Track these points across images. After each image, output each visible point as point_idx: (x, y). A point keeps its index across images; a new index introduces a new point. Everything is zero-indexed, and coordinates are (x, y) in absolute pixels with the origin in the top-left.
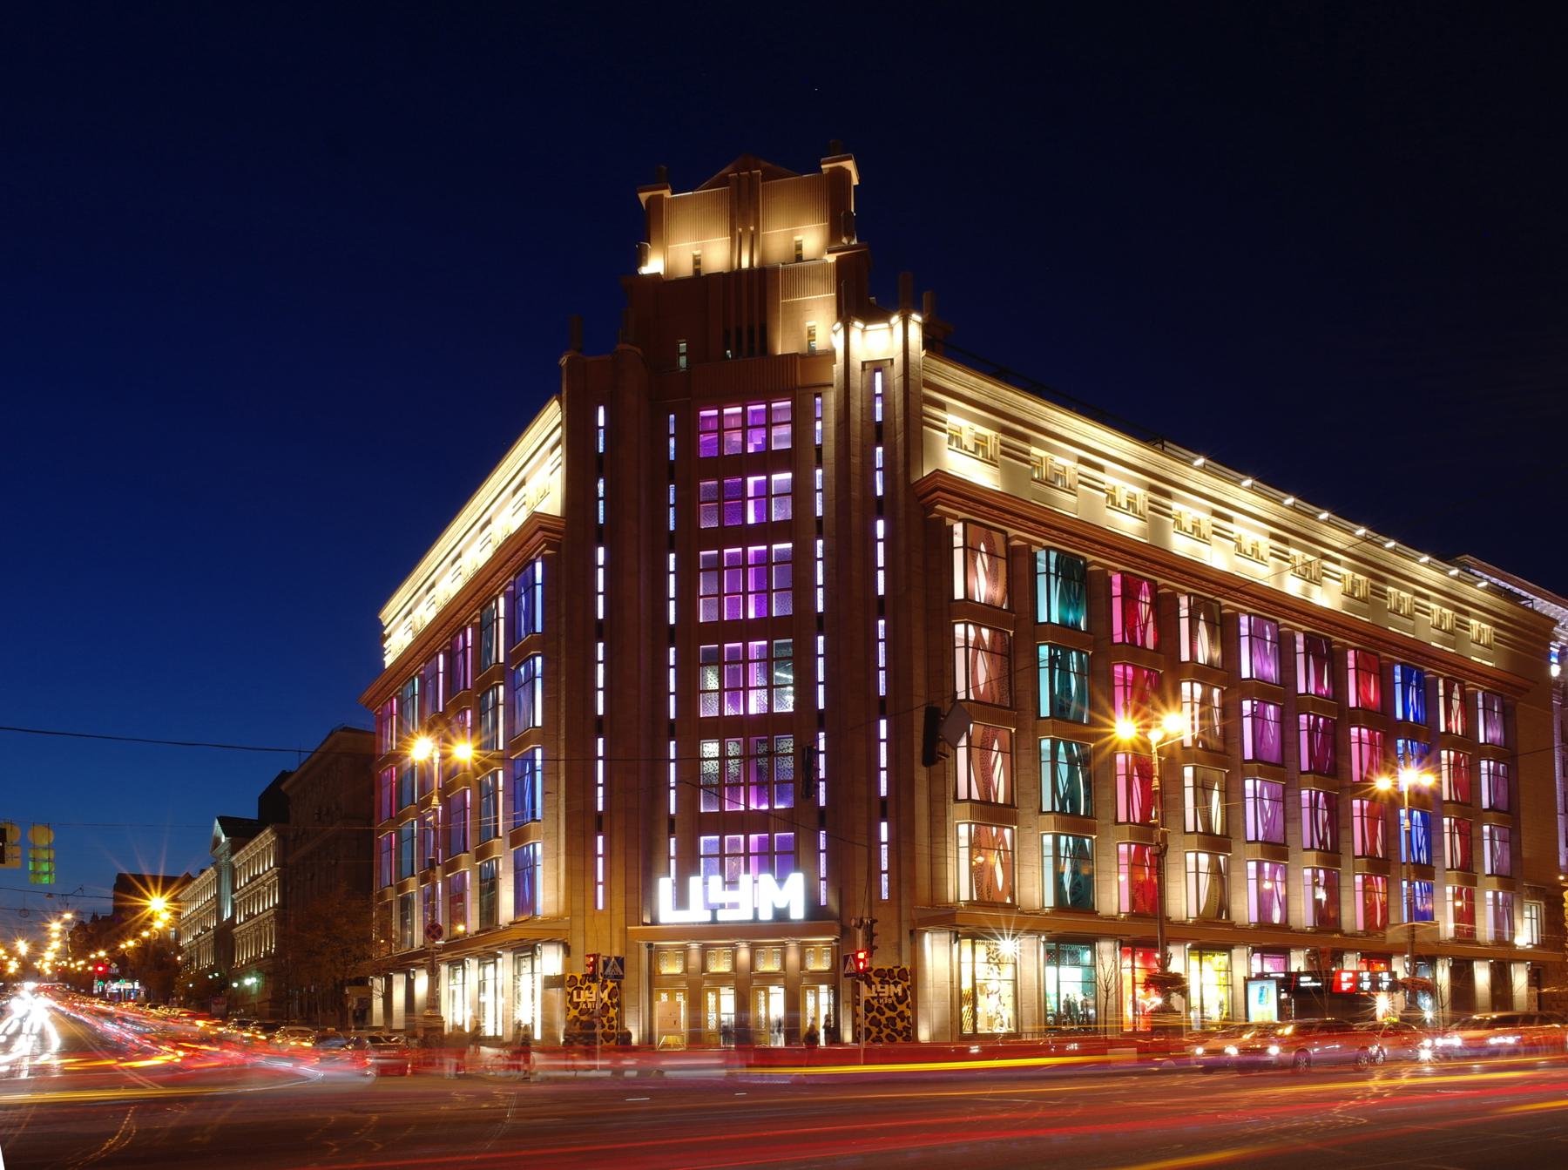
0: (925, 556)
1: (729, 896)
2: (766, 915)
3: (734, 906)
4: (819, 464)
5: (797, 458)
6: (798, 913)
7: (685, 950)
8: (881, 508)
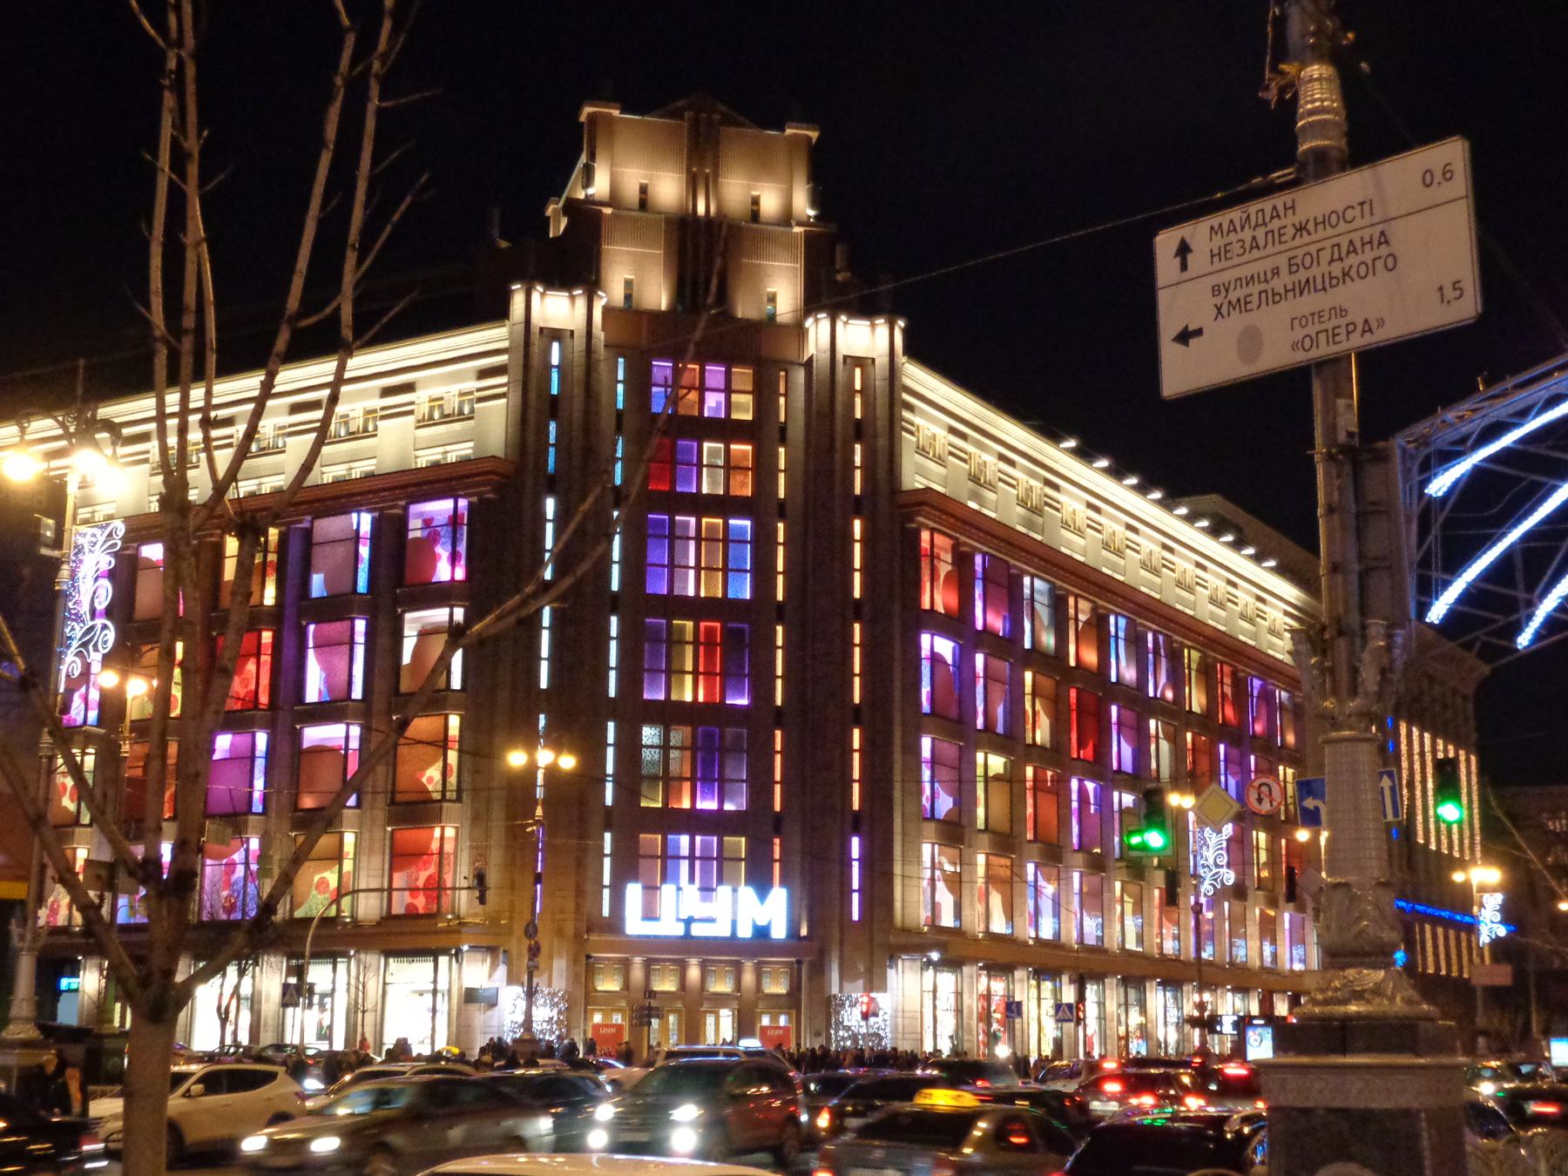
0: (898, 564)
2: (745, 932)
3: (711, 920)
4: (783, 440)
5: (760, 431)
6: (779, 932)
7: (626, 965)
8: (858, 506)
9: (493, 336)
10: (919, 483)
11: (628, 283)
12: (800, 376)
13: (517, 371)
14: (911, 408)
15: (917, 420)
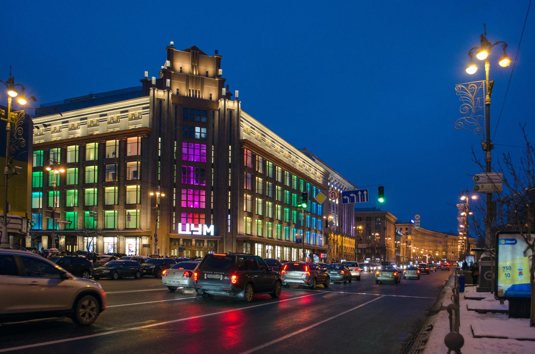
1: (196, 229)
2: (205, 234)
3: (197, 231)
6: (212, 234)
9: (145, 100)
10: (244, 138)
11: (178, 90)
12: (217, 113)
13: (152, 108)
14: (242, 121)
15: (244, 124)
